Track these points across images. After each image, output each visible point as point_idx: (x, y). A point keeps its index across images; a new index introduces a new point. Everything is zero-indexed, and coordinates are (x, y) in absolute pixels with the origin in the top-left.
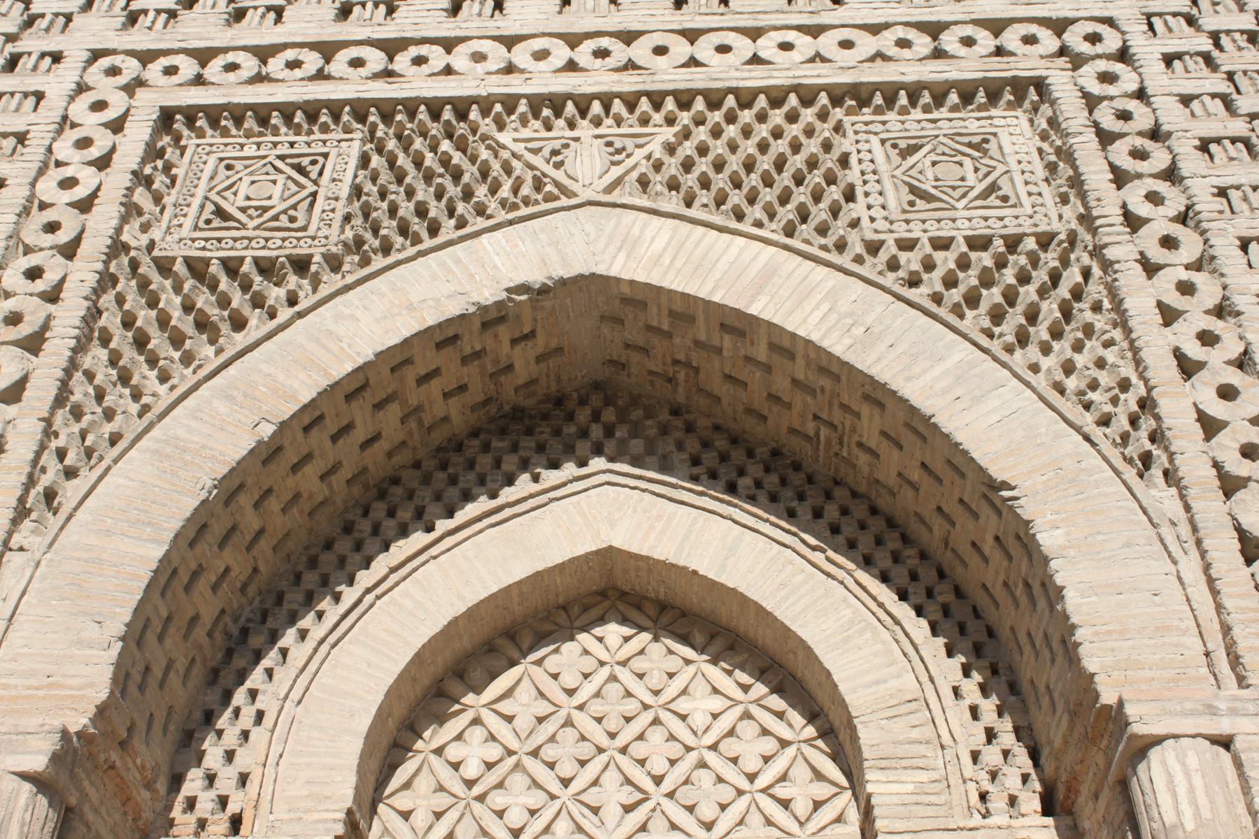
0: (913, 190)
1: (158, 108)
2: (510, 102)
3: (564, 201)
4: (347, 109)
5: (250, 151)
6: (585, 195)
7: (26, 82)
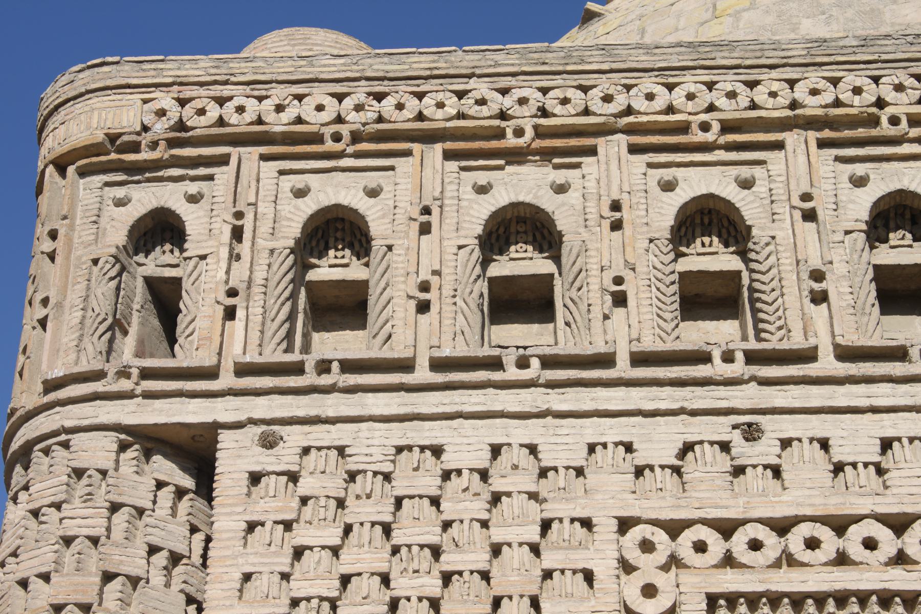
1: (704, 596)
4: (874, 598)
7: (572, 557)
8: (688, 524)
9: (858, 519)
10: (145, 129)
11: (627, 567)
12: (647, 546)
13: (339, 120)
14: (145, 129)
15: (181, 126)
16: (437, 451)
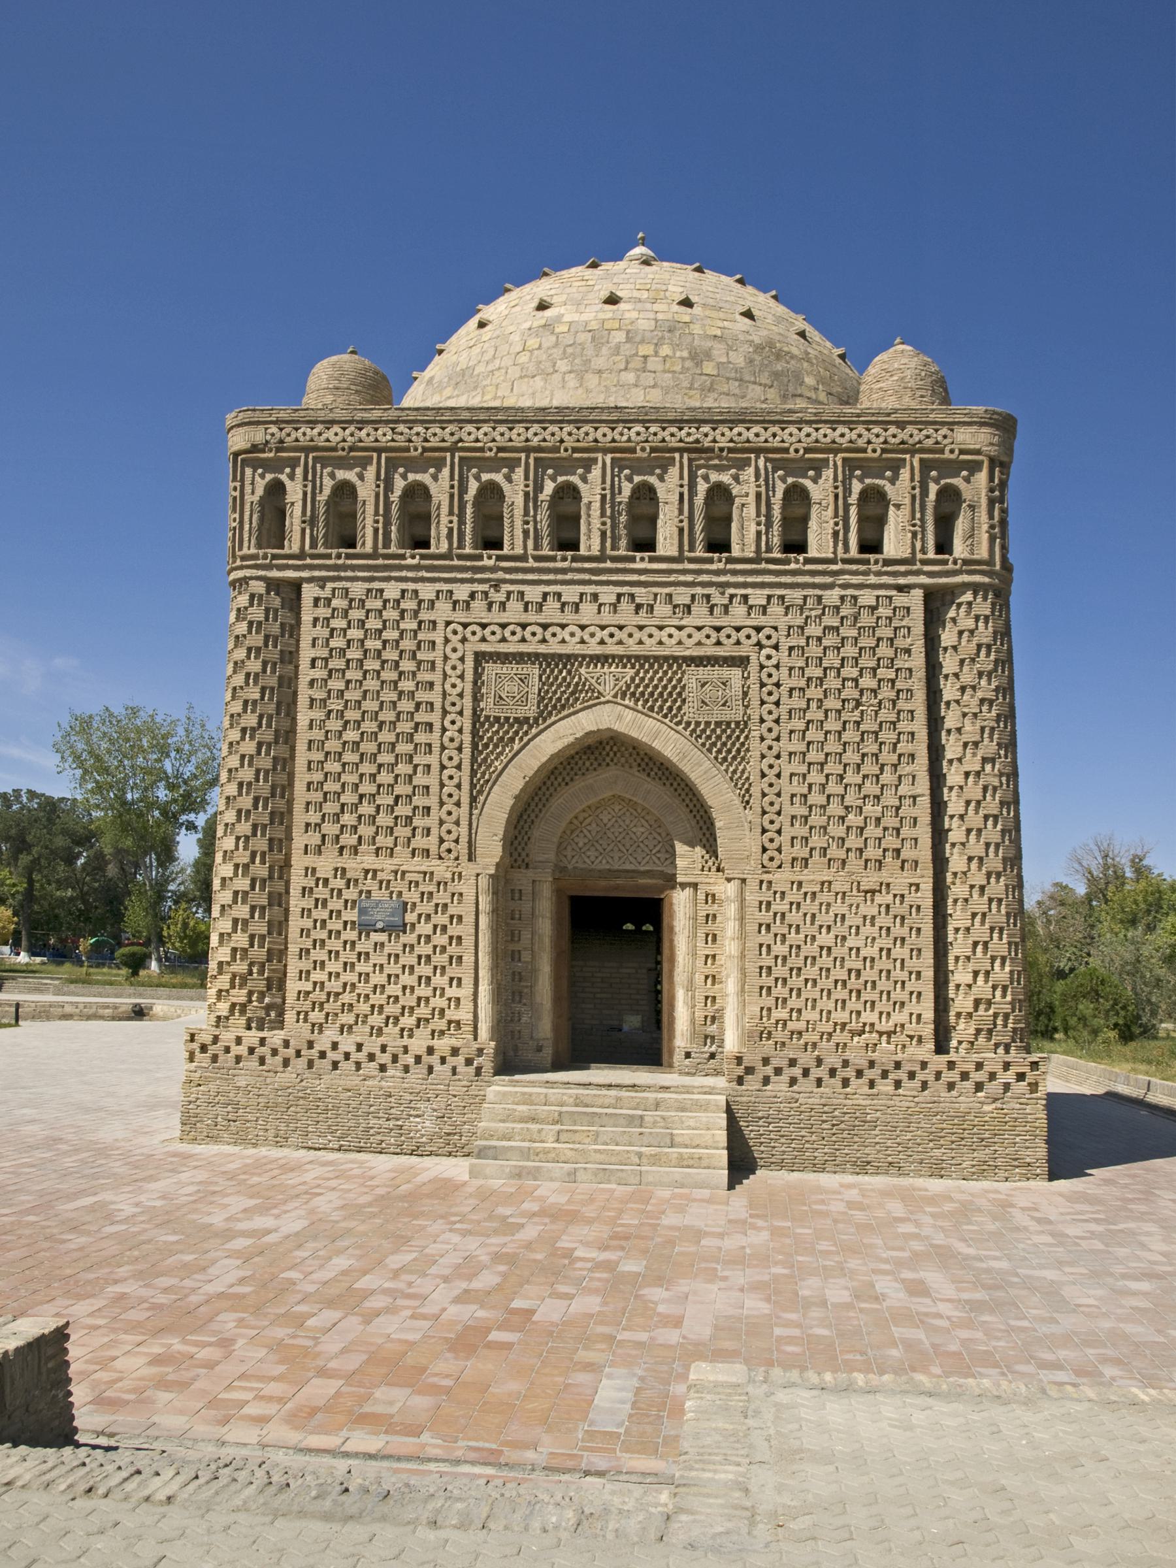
0: (703, 702)
2: (584, 657)
3: (602, 699)
5: (504, 671)
6: (609, 698)
8: (470, 624)
9: (530, 624)
10: (267, 442)
11: (447, 641)
12: (455, 632)
13: (344, 440)
14: (267, 442)
15: (281, 441)
16: (382, 591)
